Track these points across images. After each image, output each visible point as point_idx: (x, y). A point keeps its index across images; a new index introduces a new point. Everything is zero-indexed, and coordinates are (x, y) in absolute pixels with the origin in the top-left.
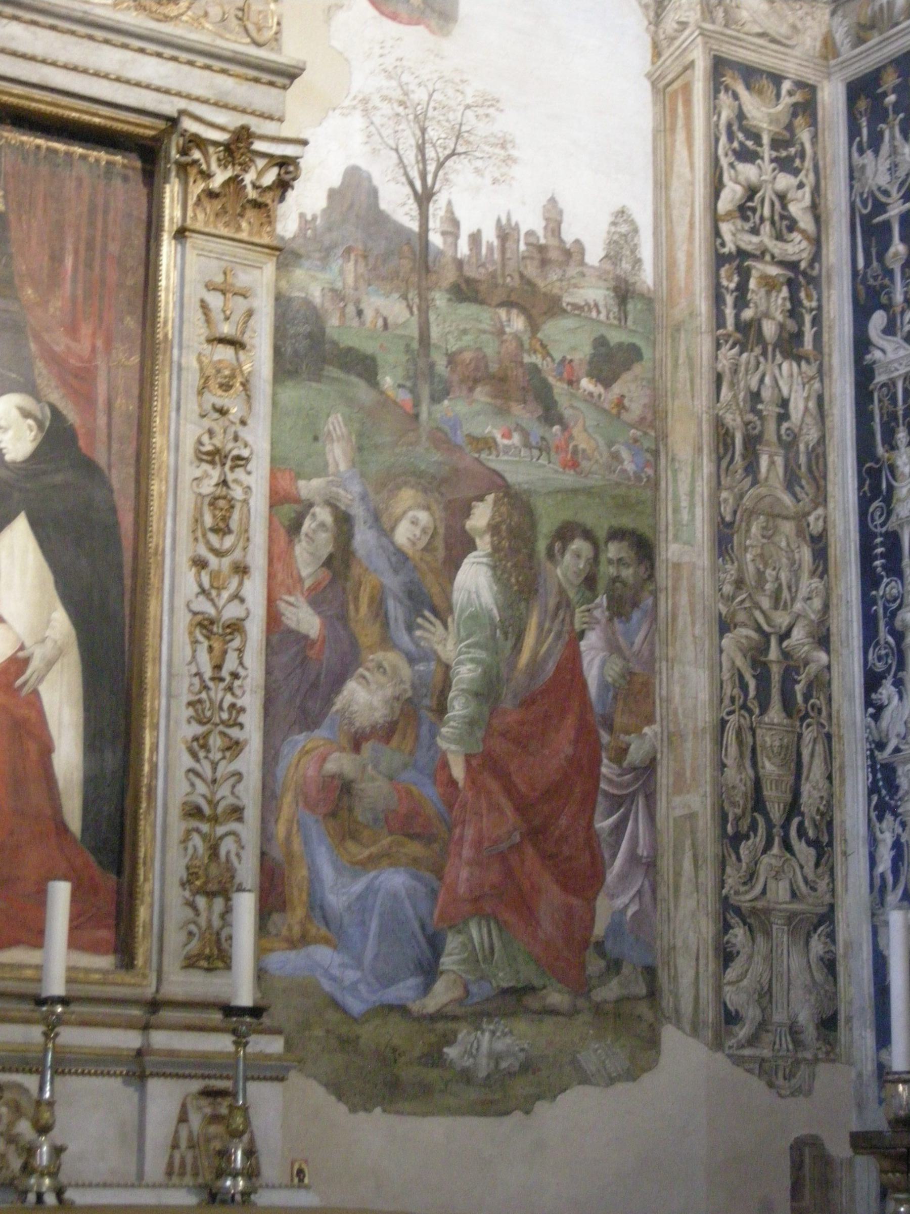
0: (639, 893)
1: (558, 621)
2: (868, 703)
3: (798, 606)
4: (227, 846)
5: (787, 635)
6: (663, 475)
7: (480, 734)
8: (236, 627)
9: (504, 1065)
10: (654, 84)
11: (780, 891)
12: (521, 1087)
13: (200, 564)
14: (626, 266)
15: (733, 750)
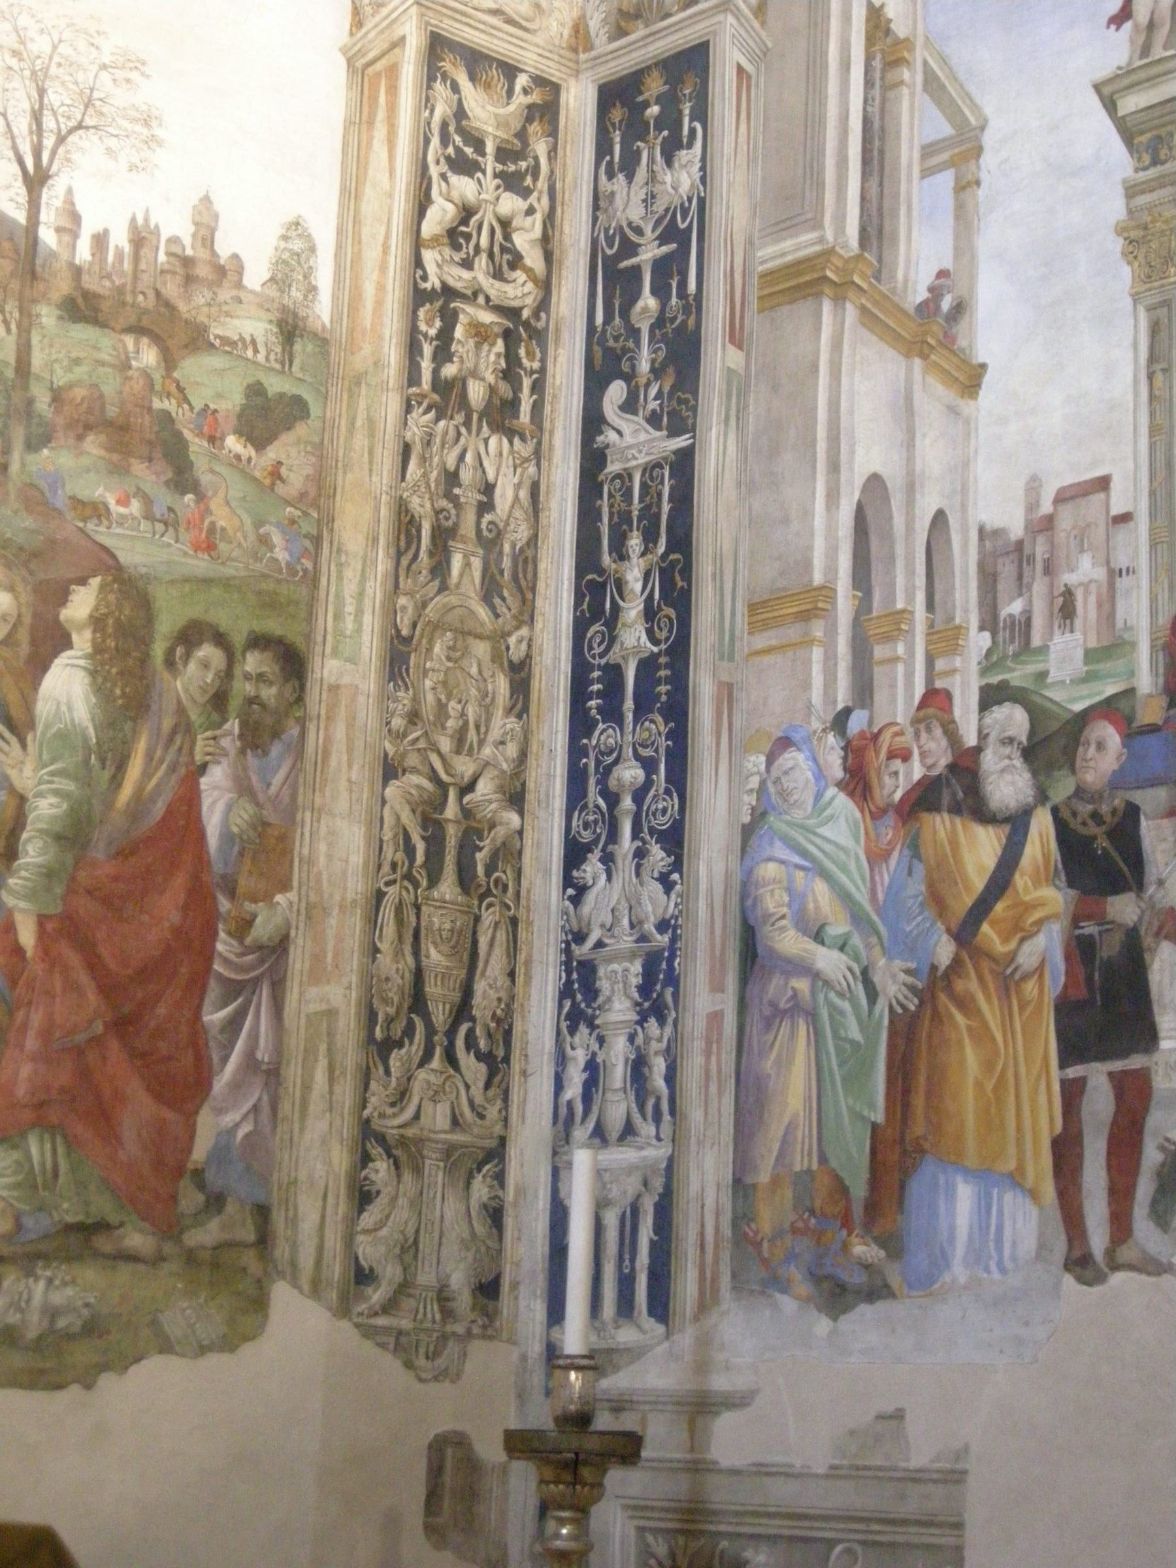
0: (255, 1108)
1: (173, 749)
2: (568, 881)
3: (487, 751)
5: (470, 787)
6: (324, 569)
7: (59, 890)
9: (61, 1323)
10: (350, 62)
11: (438, 1117)
12: (82, 1354)
14: (296, 294)
15: (390, 930)
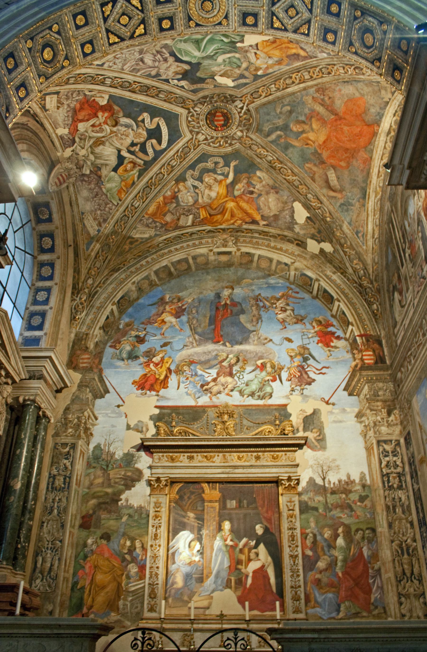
4: (299, 592)
5: (406, 541)
8: (297, 556)
11: (412, 590)
13: (290, 546)
15: (397, 564)
